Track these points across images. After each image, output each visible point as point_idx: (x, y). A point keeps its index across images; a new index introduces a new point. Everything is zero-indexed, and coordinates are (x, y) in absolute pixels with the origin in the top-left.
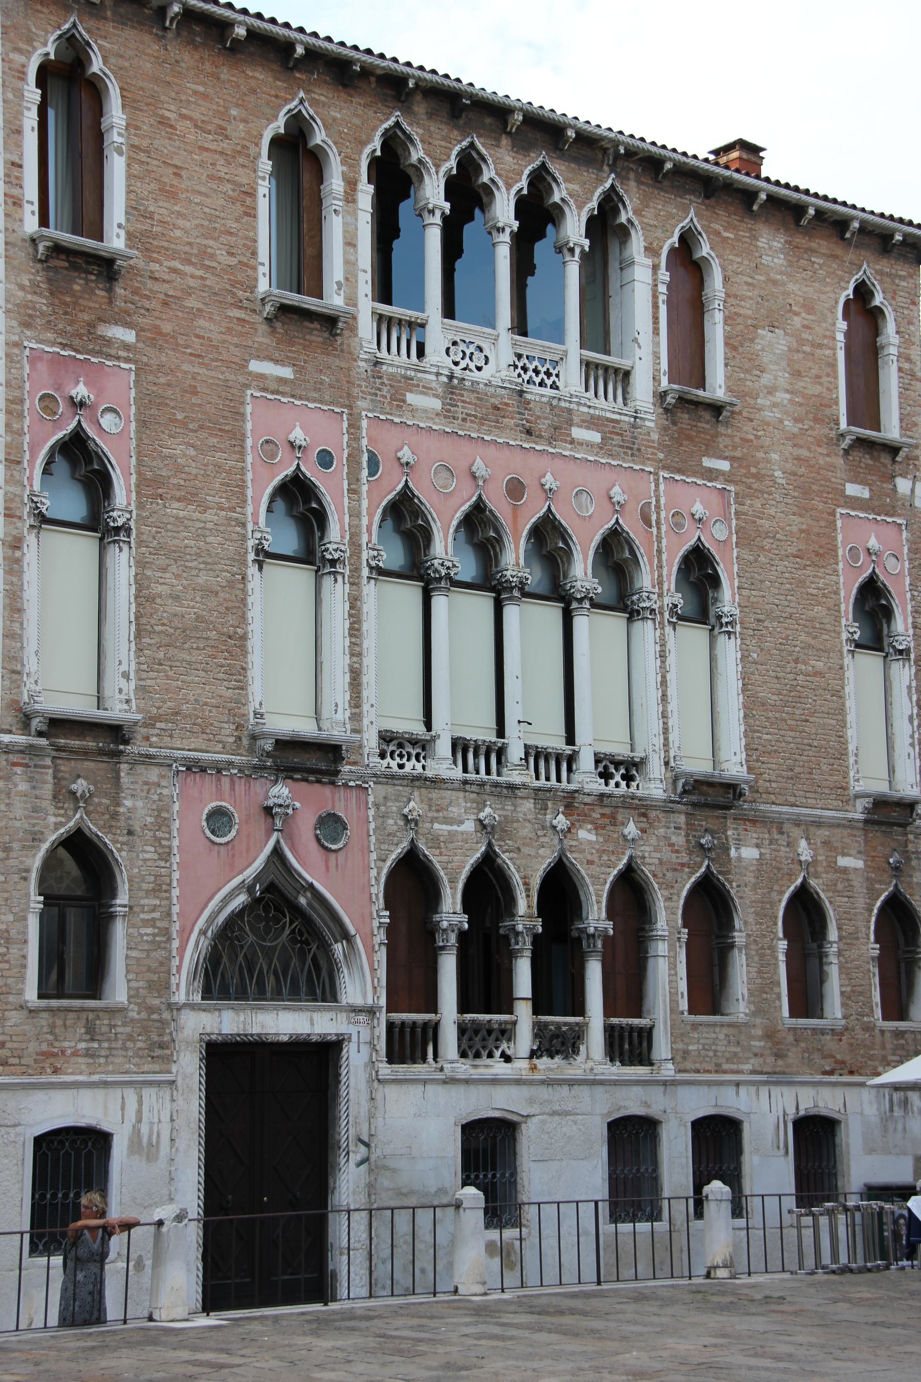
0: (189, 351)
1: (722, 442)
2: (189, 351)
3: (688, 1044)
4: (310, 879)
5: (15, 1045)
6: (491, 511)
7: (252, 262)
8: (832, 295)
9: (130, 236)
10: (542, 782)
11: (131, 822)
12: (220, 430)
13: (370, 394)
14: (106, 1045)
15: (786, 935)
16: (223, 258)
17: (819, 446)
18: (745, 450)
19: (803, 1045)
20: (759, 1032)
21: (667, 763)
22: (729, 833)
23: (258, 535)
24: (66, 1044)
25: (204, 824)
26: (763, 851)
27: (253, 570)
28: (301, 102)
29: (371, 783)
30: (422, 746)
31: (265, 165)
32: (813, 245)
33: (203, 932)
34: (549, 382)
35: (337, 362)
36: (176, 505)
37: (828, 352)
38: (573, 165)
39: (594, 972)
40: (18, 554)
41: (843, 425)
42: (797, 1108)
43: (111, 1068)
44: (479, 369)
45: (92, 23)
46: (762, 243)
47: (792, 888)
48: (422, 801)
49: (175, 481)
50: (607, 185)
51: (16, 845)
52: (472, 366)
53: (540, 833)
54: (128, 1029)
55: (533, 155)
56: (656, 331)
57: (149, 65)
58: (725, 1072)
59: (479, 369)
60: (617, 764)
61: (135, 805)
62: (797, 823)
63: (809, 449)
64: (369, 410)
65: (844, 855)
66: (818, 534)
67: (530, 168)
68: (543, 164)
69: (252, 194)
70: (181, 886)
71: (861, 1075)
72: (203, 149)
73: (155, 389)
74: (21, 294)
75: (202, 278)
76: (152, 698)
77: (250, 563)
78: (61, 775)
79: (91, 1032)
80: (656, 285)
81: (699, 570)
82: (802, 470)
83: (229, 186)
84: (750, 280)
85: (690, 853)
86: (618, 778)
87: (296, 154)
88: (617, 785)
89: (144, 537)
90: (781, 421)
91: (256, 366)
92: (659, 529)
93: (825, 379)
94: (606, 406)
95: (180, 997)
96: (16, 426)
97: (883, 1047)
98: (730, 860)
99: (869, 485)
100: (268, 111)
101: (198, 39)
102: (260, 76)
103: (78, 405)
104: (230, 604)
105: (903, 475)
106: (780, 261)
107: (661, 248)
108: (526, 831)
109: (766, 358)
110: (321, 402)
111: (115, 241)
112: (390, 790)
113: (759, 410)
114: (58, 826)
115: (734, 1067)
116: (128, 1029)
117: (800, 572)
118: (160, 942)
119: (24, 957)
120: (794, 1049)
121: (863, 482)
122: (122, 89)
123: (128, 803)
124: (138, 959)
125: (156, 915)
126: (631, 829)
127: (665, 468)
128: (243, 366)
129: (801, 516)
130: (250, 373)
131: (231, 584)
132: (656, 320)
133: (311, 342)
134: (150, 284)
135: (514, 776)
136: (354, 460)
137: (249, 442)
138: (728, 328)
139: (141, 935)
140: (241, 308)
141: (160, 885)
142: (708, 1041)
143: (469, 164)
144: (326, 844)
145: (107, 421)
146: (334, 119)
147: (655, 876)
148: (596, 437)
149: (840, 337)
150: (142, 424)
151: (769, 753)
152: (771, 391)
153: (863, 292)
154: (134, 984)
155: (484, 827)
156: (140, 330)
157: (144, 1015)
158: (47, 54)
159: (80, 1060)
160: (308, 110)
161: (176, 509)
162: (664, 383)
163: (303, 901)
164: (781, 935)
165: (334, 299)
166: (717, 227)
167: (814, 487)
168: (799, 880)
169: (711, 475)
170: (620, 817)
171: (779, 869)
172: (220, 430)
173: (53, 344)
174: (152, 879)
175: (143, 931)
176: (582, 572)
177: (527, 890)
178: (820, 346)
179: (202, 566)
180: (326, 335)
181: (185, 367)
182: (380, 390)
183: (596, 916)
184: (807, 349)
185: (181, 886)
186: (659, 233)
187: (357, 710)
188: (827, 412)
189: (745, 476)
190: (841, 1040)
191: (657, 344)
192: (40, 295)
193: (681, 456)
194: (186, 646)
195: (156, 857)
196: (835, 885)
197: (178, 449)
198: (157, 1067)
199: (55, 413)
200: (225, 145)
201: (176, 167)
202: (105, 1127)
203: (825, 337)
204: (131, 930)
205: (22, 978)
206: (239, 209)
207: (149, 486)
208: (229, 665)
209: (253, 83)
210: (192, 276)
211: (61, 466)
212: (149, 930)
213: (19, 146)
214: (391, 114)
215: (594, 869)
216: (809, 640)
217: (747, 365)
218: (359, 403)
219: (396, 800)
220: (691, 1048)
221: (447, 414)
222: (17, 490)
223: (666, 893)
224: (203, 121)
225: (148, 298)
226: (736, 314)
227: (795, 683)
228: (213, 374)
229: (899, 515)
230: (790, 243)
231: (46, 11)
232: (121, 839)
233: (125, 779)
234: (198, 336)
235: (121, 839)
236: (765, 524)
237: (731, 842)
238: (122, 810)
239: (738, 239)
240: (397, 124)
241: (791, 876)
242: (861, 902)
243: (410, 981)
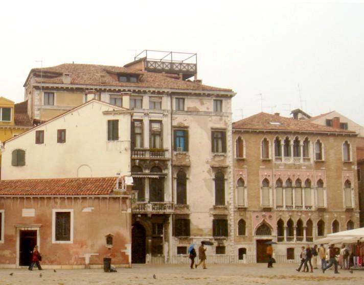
30: (282, 207)
31: (261, 144)
39: (305, 232)
62: (335, 212)
69: (260, 148)
70: (253, 223)
79: (244, 239)
81: (320, 183)
87: (266, 142)
94: (306, 163)
95: (253, 235)
102: (260, 135)
103: (241, 175)
111: (244, 157)
126: (310, 214)
135: (294, 209)
136: (273, 174)
143: (287, 139)
148: (305, 168)
150: (248, 175)
160: (266, 137)
162: (315, 159)
165: (270, 158)
169: (322, 170)
176: (303, 184)
183: (305, 225)
185: (253, 223)
207: (249, 182)
211: (239, 181)
221: (285, 168)
243: (280, 232)
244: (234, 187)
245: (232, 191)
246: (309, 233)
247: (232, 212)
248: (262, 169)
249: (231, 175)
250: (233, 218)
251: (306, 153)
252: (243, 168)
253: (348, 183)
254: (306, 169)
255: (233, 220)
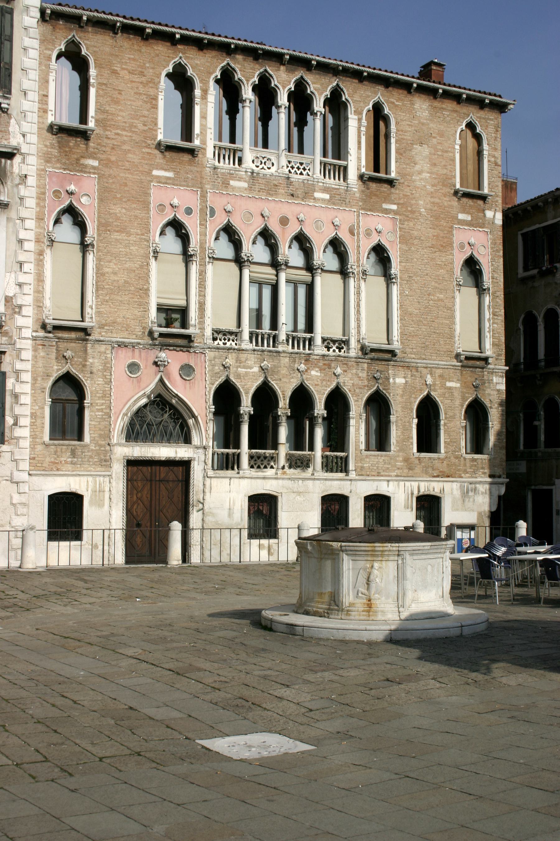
0: (123, 168)
1: (393, 197)
2: (123, 168)
3: (363, 464)
4: (176, 392)
5: (40, 459)
6: (271, 231)
7: (155, 128)
8: (453, 129)
9: (97, 121)
10: (296, 350)
11: (92, 368)
12: (138, 201)
13: (212, 182)
14: (80, 460)
15: (418, 417)
16: (141, 127)
17: (445, 197)
18: (405, 200)
19: (423, 464)
20: (401, 459)
21: (359, 341)
22: (390, 372)
23: (154, 245)
24: (62, 459)
25: (127, 369)
26: (407, 380)
27: (152, 260)
28: (181, 58)
29: (207, 351)
32: (444, 106)
33: (126, 414)
34: (304, 173)
35: (196, 168)
36: (116, 234)
37: (450, 154)
38: (317, 76)
39: (319, 433)
40: (41, 257)
41: (458, 186)
42: (419, 491)
43: (82, 469)
44: (269, 168)
45: (82, 35)
46: (417, 106)
47: (422, 396)
48: (232, 359)
49: (115, 223)
50: (335, 84)
51: (39, 379)
52: (265, 167)
53: (291, 372)
54: (90, 454)
55: (296, 73)
56: (359, 148)
57: (107, 49)
58: (382, 476)
59: (269, 168)
60: (334, 342)
61: (94, 361)
63: (440, 199)
64: (211, 189)
65: (450, 381)
66: (443, 237)
67: (295, 79)
68: (302, 77)
69: (156, 99)
71: (452, 477)
72: (132, 82)
73: (107, 185)
74: (45, 149)
75: (130, 136)
76: (103, 316)
77: (151, 258)
78: (60, 349)
79: (73, 453)
80: (360, 127)
82: (436, 208)
83: (145, 96)
84: (410, 123)
85: (369, 380)
86: (334, 348)
88: (334, 351)
89: (101, 248)
90: (425, 186)
91: (155, 173)
92: (358, 237)
93: (449, 167)
94: (331, 182)
95: (115, 441)
96: (42, 204)
97: (465, 465)
98: (389, 384)
99: (471, 214)
100: (164, 63)
101: (131, 36)
103: (71, 194)
104: (141, 275)
105: (490, 209)
106: (426, 114)
107: (363, 111)
108: (284, 371)
109: (417, 158)
110: (187, 186)
112: (217, 353)
113: (414, 182)
114: (58, 370)
115: (386, 474)
116: (90, 454)
117: (433, 254)
118: (105, 418)
119: (43, 423)
120: (419, 466)
121: (468, 213)
122: (95, 60)
123: (91, 360)
124: (95, 425)
125: (104, 407)
127: (362, 209)
128: (149, 173)
129: (434, 229)
130: (153, 176)
131: (141, 267)
132: (359, 143)
133: (183, 161)
134: (105, 140)
135: (280, 348)
137: (152, 205)
138: (398, 145)
139: (97, 416)
140: (149, 148)
141: (105, 395)
142: (374, 463)
144: (184, 377)
145: (84, 200)
146: (197, 64)
147: (350, 391)
148: (327, 196)
149: (457, 147)
150: (101, 200)
151: (413, 336)
152: (420, 173)
153: (471, 126)
154: (93, 435)
155: (263, 370)
156: (100, 160)
157: (97, 448)
158: (61, 49)
159: (68, 465)
160: (184, 61)
161: (116, 236)
163: (174, 401)
164: (415, 416)
166: (392, 100)
167: (442, 216)
168: (425, 393)
169: (387, 211)
170: (333, 365)
171: (415, 388)
172: (138, 201)
173: (60, 169)
174: (102, 392)
175: (97, 413)
177: (284, 397)
178: (447, 152)
179: (128, 259)
180: (191, 157)
181: (122, 175)
182: (216, 180)
184: (440, 153)
186: (362, 104)
187: (201, 320)
188: (450, 181)
189: (405, 211)
190: (443, 462)
191: (359, 154)
192: (55, 148)
193: (370, 205)
194: (119, 294)
195: (104, 383)
196: (445, 395)
197: (117, 209)
198: (104, 469)
199: (60, 198)
200: (144, 79)
201: (120, 90)
202: (79, 492)
203: (449, 147)
204: (91, 413)
205: (42, 432)
206: (149, 105)
207: (103, 226)
208: (140, 302)
209: (157, 52)
210: (126, 136)
212: (100, 413)
213: (47, 88)
214: (225, 60)
215: (319, 388)
216: (437, 285)
217: (408, 162)
218: (206, 186)
219: (219, 358)
220: (365, 465)
221: (250, 189)
222: (42, 231)
223: (355, 398)
224: (133, 70)
225: (105, 146)
226: (402, 138)
227: (428, 304)
228: (135, 177)
229: (487, 228)
230: (432, 106)
231: (61, 32)
232: (87, 375)
233: (90, 351)
234: (128, 161)
235: (87, 375)
236: (415, 233)
237: (391, 376)
238: (88, 363)
239: (403, 105)
240: (228, 64)
241: (421, 390)
242: (458, 402)
243: (228, 436)
244: (38, 241)
245: (31, 257)
246: (337, 438)
247: (28, 344)
248: (159, 179)
249: (29, 191)
250: (28, 366)
251: (337, 145)
252: (83, 169)
253: (472, 266)
254: (329, 201)
255: (26, 377)
